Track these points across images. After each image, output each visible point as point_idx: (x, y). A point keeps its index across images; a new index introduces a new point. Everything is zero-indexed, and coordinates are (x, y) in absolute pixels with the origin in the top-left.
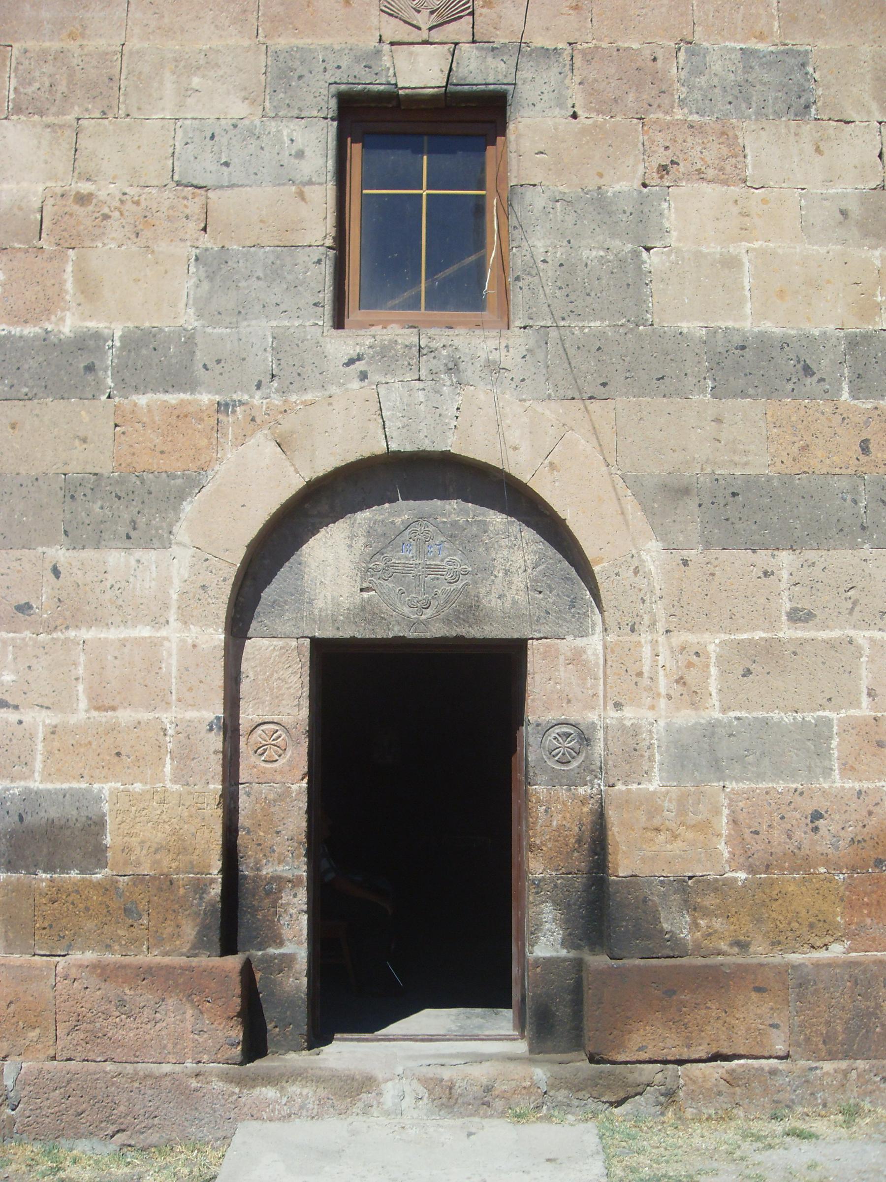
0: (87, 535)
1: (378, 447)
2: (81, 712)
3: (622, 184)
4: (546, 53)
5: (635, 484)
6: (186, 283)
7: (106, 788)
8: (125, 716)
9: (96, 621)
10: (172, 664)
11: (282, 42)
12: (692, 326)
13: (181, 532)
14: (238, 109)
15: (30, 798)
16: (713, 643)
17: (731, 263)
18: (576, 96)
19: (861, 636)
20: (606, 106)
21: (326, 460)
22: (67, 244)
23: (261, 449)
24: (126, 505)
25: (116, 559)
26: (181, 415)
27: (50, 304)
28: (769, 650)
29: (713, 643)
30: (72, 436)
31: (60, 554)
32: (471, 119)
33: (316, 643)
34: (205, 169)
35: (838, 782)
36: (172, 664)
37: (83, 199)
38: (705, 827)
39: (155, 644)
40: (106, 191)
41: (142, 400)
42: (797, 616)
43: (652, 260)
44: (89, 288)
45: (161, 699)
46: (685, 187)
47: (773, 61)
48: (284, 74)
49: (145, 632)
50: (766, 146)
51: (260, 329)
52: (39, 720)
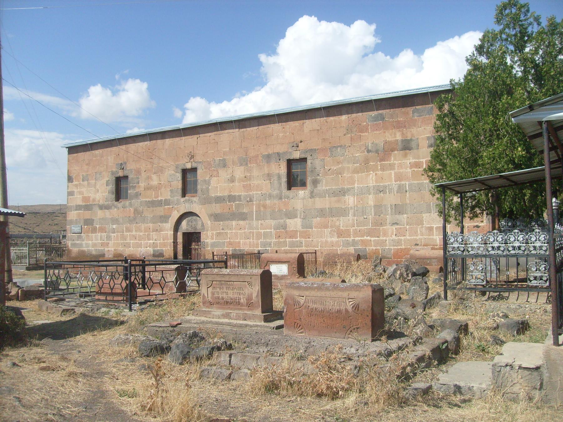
0: (162, 222)
2: (162, 241)
4: (200, 162)
12: (213, 195)
14: (173, 172)
16: (214, 232)
17: (217, 187)
18: (203, 167)
22: (159, 189)
23: (176, 212)
24: (164, 219)
26: (169, 208)
27: (158, 197)
28: (219, 233)
29: (214, 232)
30: (160, 211)
31: (160, 224)
32: (194, 170)
34: (170, 180)
42: (222, 229)
43: (210, 187)
47: (222, 160)
50: (220, 172)
51: (176, 198)
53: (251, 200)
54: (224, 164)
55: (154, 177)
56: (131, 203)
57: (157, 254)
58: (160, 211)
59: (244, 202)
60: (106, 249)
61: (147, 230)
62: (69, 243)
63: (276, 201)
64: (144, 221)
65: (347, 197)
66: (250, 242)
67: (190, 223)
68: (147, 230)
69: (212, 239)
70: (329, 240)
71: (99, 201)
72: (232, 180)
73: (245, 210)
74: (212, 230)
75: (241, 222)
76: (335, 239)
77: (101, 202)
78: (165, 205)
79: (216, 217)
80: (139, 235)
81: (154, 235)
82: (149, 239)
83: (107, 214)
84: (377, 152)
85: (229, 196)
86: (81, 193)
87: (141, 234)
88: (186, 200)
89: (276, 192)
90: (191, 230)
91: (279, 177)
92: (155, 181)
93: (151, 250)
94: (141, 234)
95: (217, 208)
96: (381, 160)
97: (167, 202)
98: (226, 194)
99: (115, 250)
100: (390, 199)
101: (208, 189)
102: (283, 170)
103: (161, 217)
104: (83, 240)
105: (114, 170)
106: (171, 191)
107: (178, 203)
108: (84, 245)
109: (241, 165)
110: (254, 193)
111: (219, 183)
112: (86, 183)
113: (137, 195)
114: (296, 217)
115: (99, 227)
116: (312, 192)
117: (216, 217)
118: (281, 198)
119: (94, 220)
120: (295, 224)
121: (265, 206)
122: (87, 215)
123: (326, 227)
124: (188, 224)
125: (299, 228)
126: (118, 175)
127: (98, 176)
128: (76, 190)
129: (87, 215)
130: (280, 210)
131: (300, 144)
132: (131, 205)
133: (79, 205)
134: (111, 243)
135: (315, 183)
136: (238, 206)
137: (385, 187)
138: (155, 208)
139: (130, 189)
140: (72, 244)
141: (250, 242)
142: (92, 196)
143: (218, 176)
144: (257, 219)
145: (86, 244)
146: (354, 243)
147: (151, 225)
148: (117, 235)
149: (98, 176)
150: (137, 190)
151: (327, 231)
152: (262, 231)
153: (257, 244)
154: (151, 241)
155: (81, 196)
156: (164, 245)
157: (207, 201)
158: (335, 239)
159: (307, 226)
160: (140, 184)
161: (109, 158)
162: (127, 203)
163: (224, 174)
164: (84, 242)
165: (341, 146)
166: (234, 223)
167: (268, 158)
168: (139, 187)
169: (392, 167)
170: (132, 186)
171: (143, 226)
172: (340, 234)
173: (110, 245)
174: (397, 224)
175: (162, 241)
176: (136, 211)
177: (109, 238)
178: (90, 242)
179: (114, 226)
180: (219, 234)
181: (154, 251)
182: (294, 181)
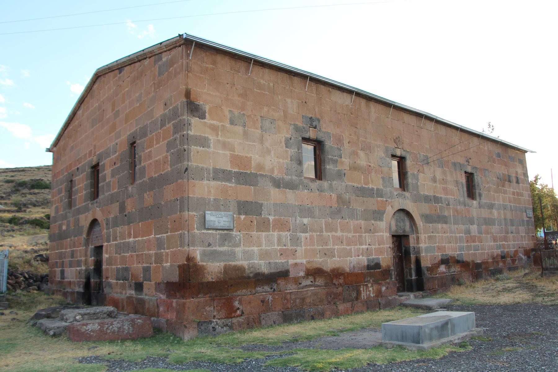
0: (375, 219)
1: (400, 208)
3: (416, 173)
5: (419, 214)
6: (381, 181)
7: (380, 257)
8: (381, 246)
9: (377, 232)
10: (385, 238)
11: (386, 145)
13: (384, 220)
14: (383, 155)
15: (373, 259)
16: (426, 235)
17: (424, 185)
19: (437, 235)
20: (414, 161)
21: (396, 210)
25: (378, 222)
26: (382, 201)
30: (372, 203)
31: (373, 222)
33: (393, 236)
35: (436, 254)
36: (385, 238)
37: (370, 166)
38: (427, 260)
39: (383, 235)
40: (372, 165)
41: (379, 199)
42: (432, 232)
43: (419, 183)
44: (372, 181)
45: (384, 244)
46: (420, 174)
48: (387, 150)
49: (382, 234)
51: (388, 189)
52: (373, 247)
53: (448, 205)
54: (426, 161)
55: (361, 154)
56: (331, 185)
57: (373, 264)
58: (372, 203)
59: (444, 205)
60: (291, 262)
61: (358, 229)
62: (197, 253)
63: (463, 207)
64: (353, 215)
65: (494, 210)
66: (452, 246)
67: (399, 223)
68: (358, 229)
69: (425, 243)
70: (490, 244)
71: (272, 170)
72: (434, 180)
73: (446, 214)
74: (425, 233)
75: (444, 226)
76: (492, 243)
77: (276, 174)
78: (377, 197)
79: (428, 218)
80: (347, 238)
81: (367, 237)
82: (361, 244)
83: (291, 197)
84: (500, 179)
85: (434, 196)
86: (225, 145)
87: (350, 235)
88: (399, 194)
89: (462, 199)
90: (400, 233)
91: (462, 186)
92: (362, 161)
93: (364, 260)
94: (350, 235)
95: (425, 208)
96: (503, 186)
97: (380, 193)
98: (431, 194)
99: (308, 262)
100: (509, 216)
101: (418, 187)
102: (463, 180)
103: (374, 212)
104: (238, 245)
105: (300, 124)
106: (383, 178)
107: (391, 197)
108: (240, 255)
109: (439, 167)
110: (450, 197)
111: (425, 181)
112: (239, 129)
113: (340, 175)
114: (474, 224)
115: (274, 220)
116: (479, 203)
117: (428, 218)
118: (465, 206)
119: (261, 205)
120: (474, 228)
121: (457, 211)
122: (247, 193)
123: (488, 234)
124: (397, 225)
125: (477, 234)
126: (307, 136)
127: (267, 124)
128: (212, 138)
129: (247, 193)
130: (466, 216)
131: (470, 161)
132: (331, 186)
133: (224, 171)
134: (301, 250)
135: (480, 195)
136: (441, 208)
137: (506, 205)
138: (365, 199)
139: (329, 163)
140: (204, 254)
141: (452, 246)
142: (256, 158)
143: (424, 173)
144: (454, 224)
145: (245, 252)
146: (499, 247)
147: (363, 222)
148: (312, 237)
149: (267, 124)
150: (339, 167)
151: (489, 236)
152: (458, 235)
153: (456, 248)
154: (364, 247)
155: (228, 153)
156: (381, 251)
157: (419, 199)
158: (492, 243)
159: (480, 232)
160: (343, 159)
161: (289, 101)
162: (325, 184)
163: (428, 172)
164: (237, 249)
165: (487, 170)
166: (440, 226)
167: (455, 164)
168: (342, 163)
169: (505, 192)
170: (332, 159)
171: (352, 223)
172: (495, 240)
173: (298, 254)
174: (512, 233)
175: (377, 247)
176: (340, 198)
177: (295, 241)
178: (256, 249)
179: (306, 221)
180: (430, 237)
181: (368, 260)
182: (471, 190)
